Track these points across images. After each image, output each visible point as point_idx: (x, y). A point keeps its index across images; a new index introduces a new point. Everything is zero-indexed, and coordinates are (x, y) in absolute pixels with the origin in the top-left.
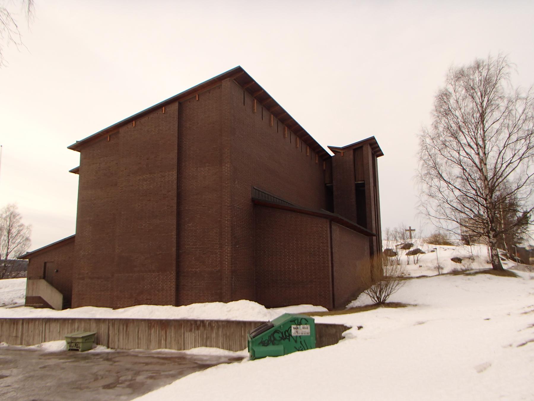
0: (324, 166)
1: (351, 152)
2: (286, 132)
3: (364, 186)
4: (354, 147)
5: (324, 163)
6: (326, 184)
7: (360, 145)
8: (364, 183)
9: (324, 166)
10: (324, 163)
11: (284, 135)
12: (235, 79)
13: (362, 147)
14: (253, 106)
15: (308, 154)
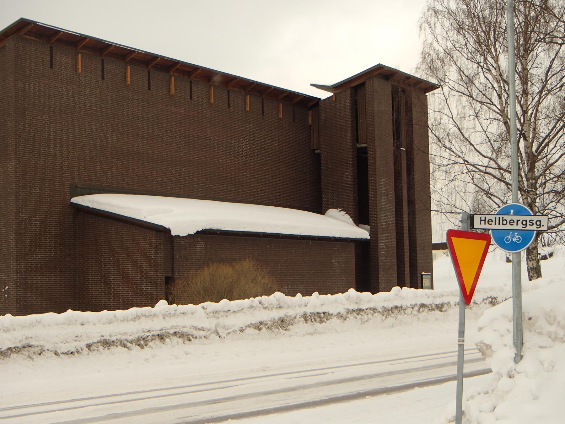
0: (310, 118)
1: (348, 93)
2: (173, 85)
3: (366, 153)
4: (353, 85)
5: (310, 113)
6: (314, 150)
7: (357, 83)
8: (366, 148)
9: (310, 118)
10: (310, 113)
11: (169, 90)
12: (25, 34)
13: (363, 84)
14: (76, 64)
15: (248, 109)
